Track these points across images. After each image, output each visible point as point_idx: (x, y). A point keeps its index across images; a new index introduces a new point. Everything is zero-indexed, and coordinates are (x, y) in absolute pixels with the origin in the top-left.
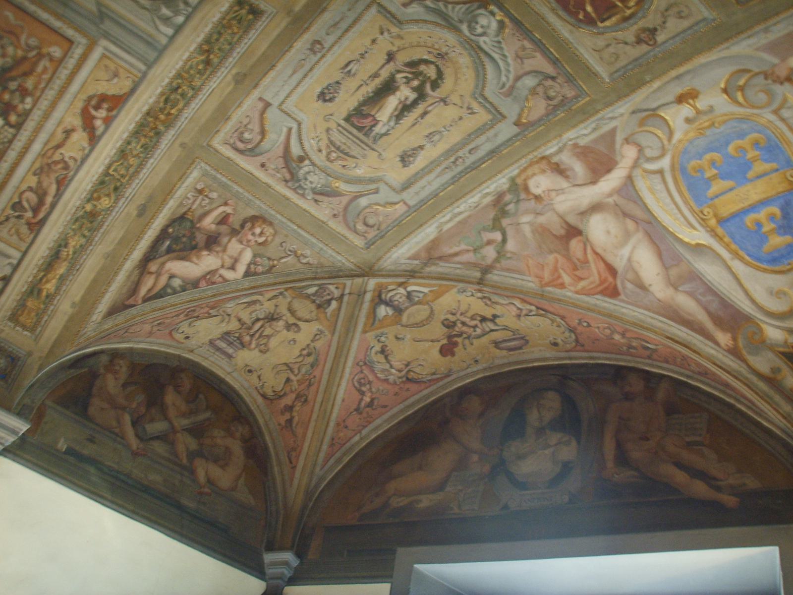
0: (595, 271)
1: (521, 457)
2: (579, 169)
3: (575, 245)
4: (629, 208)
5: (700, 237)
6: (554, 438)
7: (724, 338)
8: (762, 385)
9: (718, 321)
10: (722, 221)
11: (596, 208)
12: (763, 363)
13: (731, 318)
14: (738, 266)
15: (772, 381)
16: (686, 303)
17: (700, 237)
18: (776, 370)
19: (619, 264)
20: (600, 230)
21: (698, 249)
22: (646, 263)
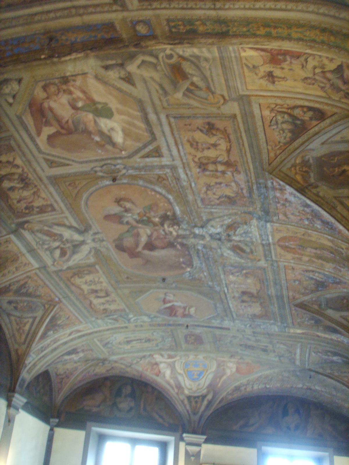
0: (156, 371)
1: (120, 403)
2: (166, 356)
3: (155, 366)
4: (172, 367)
5: (182, 372)
6: (129, 399)
7: (176, 390)
8: (180, 402)
9: (177, 387)
10: (188, 371)
11: (165, 362)
12: (182, 397)
13: (179, 387)
14: (186, 379)
15: (182, 401)
16: (172, 382)
17: (182, 372)
18: (184, 399)
19: (162, 371)
20: (162, 366)
21: (180, 374)
22: (168, 373)
